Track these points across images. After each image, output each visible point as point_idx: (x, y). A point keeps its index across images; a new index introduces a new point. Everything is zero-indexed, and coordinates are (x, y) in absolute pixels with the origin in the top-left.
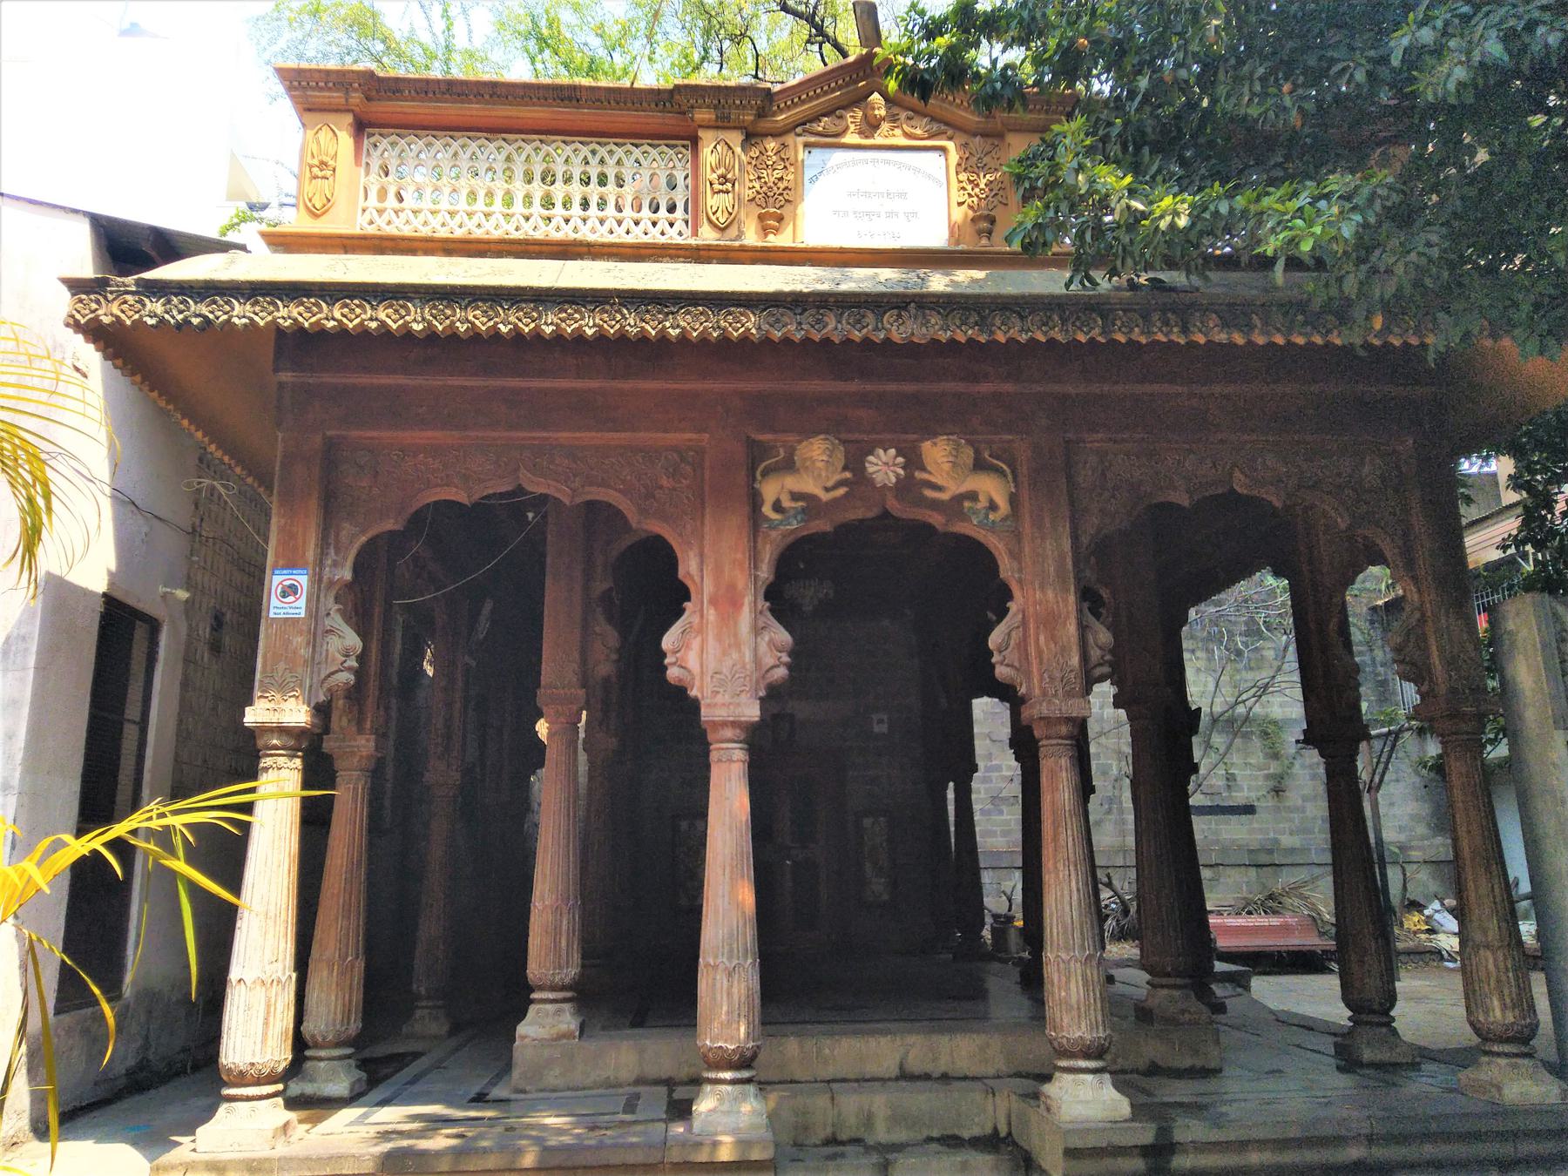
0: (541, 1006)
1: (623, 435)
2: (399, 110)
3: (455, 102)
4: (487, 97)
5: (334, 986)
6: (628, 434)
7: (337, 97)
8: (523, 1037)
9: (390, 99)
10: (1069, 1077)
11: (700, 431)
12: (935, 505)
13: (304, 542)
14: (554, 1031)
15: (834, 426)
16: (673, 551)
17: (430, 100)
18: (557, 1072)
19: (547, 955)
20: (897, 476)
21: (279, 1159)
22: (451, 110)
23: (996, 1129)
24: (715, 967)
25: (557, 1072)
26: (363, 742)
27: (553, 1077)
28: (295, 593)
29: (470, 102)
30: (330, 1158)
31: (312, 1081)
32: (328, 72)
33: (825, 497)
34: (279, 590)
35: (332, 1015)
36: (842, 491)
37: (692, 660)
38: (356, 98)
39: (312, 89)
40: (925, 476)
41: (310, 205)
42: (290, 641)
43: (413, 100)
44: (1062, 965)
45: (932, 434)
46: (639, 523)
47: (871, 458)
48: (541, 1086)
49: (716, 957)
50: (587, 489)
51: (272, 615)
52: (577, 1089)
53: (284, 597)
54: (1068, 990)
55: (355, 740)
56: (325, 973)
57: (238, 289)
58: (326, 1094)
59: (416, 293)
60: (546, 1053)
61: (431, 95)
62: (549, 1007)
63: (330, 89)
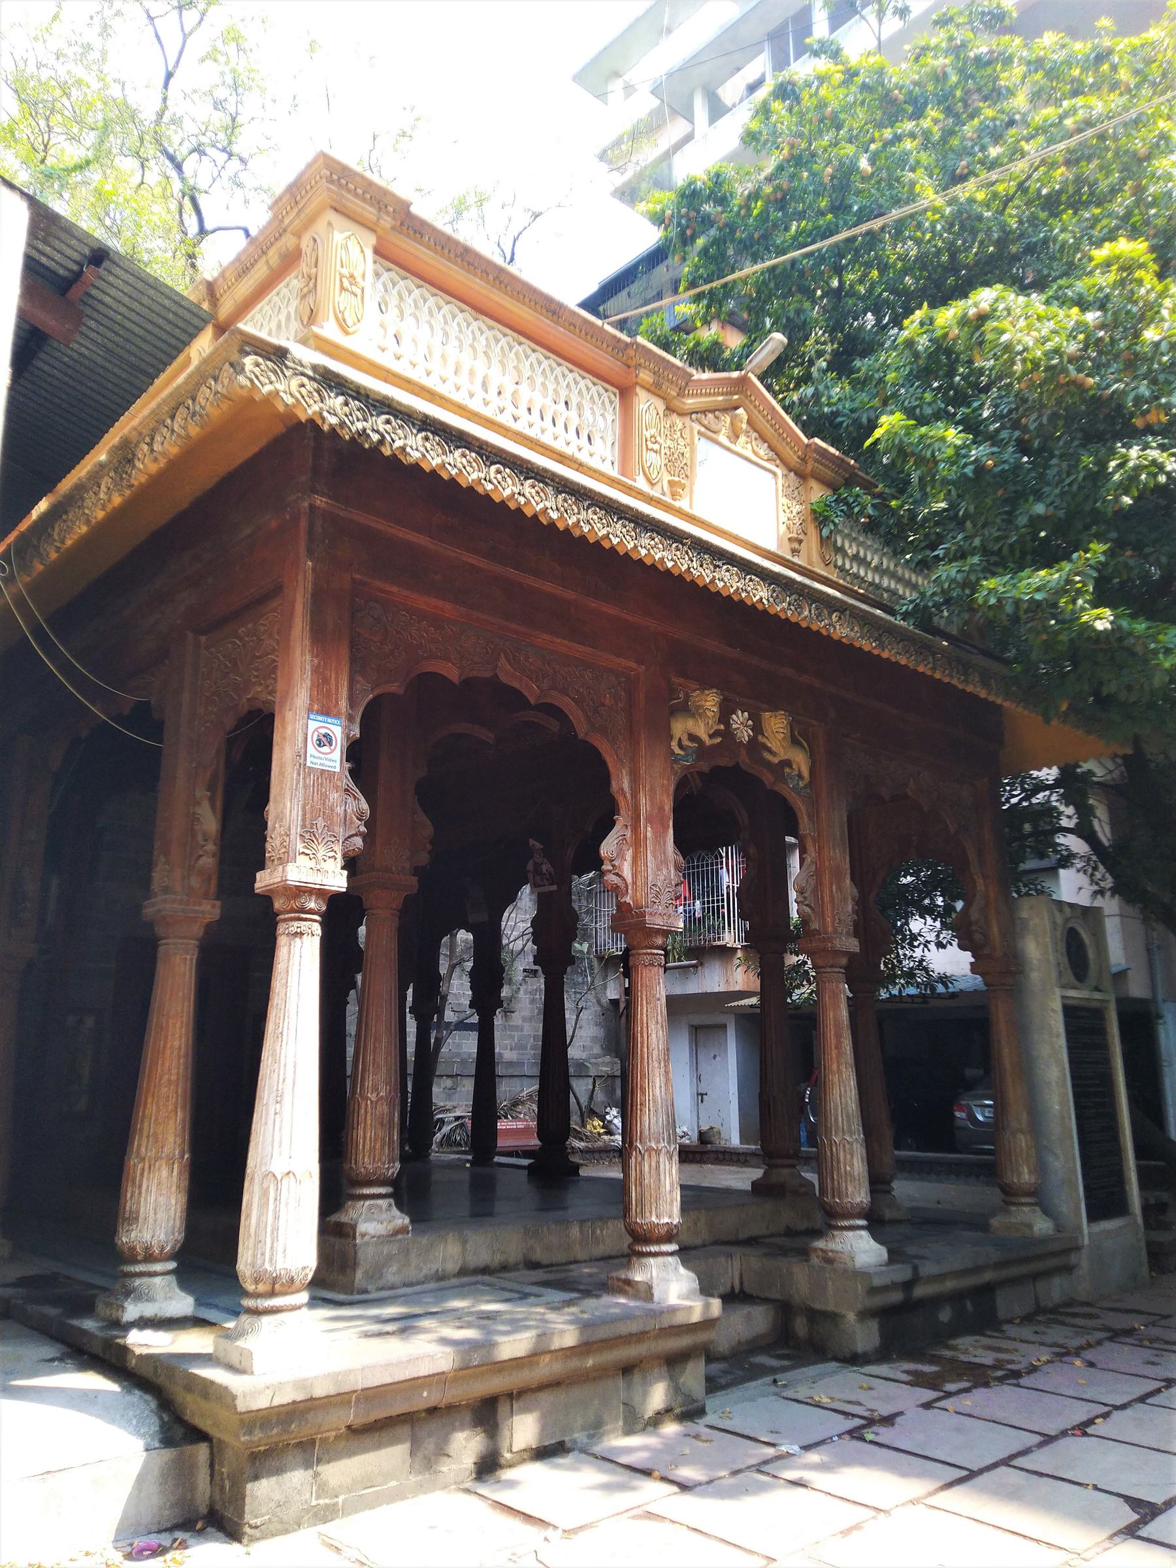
0: (372, 1202)
1: (582, 648)
2: (412, 250)
3: (462, 268)
4: (491, 277)
5: (174, 1189)
6: (589, 650)
7: (370, 212)
8: (363, 1235)
9: (408, 236)
10: (850, 1234)
11: (640, 662)
12: (768, 765)
13: (337, 690)
14: (391, 1227)
15: (722, 685)
16: (604, 764)
17: (442, 256)
18: (394, 1268)
19: (382, 1148)
20: (749, 736)
21: (363, 1369)
22: (456, 275)
23: (733, 1288)
24: (658, 1152)
25: (394, 1268)
26: (209, 907)
27: (392, 1274)
28: (330, 744)
29: (475, 275)
30: (409, 1361)
31: (150, 1299)
32: (371, 184)
33: (708, 742)
34: (315, 738)
35: (171, 1223)
36: (719, 740)
37: (627, 871)
38: (387, 222)
39: (349, 191)
40: (764, 740)
41: (340, 316)
42: (326, 796)
43: (429, 249)
44: (847, 1146)
45: (774, 708)
46: (586, 734)
47: (734, 717)
48: (381, 1283)
49: (658, 1142)
50: (553, 693)
51: (308, 764)
52: (411, 1285)
53: (319, 745)
54: (852, 1165)
55: (200, 904)
56: (165, 1173)
57: (410, 416)
58: (168, 1315)
59: (553, 480)
60: (386, 1249)
61: (446, 251)
62: (380, 1202)
63: (364, 200)
